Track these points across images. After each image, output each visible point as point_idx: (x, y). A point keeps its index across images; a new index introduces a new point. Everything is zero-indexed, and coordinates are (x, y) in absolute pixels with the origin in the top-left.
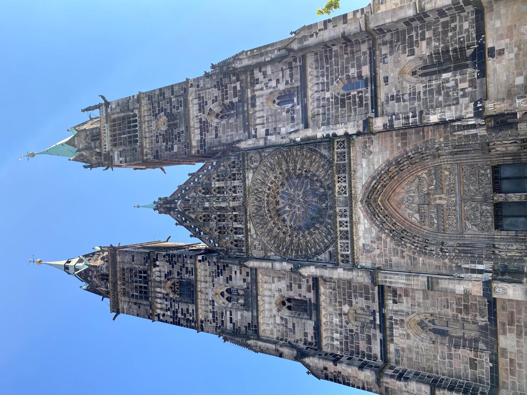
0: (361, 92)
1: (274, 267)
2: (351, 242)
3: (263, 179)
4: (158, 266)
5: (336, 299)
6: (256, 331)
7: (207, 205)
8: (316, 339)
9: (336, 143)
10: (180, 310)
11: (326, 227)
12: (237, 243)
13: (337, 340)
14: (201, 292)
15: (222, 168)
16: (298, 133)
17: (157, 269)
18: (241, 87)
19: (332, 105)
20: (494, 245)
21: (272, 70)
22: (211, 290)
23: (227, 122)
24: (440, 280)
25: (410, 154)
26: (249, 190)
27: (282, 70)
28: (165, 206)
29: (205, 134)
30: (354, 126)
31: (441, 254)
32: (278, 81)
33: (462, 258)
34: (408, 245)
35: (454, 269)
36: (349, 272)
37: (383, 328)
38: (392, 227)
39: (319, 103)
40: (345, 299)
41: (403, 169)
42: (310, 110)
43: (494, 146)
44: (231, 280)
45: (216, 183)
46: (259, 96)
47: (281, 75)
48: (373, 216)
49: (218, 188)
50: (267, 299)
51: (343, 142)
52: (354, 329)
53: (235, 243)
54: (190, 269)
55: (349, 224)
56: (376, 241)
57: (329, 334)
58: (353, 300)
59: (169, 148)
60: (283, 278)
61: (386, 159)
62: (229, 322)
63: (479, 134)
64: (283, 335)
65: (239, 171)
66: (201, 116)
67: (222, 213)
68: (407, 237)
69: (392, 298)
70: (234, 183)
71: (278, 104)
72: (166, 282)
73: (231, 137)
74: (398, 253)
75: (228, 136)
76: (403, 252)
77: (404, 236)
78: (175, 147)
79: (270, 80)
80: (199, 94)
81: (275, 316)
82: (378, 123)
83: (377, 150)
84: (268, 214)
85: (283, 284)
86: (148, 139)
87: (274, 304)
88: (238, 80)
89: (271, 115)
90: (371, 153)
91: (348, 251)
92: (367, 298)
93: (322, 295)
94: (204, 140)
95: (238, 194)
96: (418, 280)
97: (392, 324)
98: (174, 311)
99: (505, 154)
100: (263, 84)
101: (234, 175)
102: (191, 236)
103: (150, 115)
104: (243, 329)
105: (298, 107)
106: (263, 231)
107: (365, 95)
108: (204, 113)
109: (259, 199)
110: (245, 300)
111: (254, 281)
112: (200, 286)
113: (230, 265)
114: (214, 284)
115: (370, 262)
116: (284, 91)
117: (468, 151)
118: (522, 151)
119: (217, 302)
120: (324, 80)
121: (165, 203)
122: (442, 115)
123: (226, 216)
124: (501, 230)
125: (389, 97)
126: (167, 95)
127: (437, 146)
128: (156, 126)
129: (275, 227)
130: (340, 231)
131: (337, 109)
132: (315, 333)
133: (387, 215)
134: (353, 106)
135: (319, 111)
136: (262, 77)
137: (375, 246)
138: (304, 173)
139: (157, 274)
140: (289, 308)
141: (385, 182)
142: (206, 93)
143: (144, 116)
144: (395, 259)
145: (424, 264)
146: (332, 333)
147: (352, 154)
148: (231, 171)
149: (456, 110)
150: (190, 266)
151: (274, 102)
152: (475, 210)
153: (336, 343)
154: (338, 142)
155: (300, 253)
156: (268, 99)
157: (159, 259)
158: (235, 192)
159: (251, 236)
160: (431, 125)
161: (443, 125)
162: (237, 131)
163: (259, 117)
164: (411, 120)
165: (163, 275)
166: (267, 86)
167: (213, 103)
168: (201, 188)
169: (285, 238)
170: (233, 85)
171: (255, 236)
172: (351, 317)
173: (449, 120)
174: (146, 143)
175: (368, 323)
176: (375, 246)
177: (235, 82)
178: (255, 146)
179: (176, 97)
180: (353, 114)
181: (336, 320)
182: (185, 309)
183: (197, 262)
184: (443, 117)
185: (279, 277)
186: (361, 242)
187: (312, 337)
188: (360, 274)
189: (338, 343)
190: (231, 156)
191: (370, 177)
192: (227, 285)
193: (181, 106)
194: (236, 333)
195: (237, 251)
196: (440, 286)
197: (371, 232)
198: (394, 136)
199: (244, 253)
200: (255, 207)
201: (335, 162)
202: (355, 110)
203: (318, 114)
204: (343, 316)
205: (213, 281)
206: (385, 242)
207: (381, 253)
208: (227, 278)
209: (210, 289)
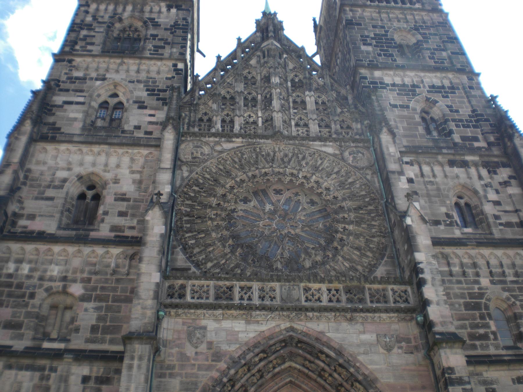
0: (496, 339)
1: (162, 171)
2: (211, 304)
4: (169, 10)
5: (96, 273)
6: (44, 138)
7: (275, 80)
8: (21, 233)
9: (403, 288)
10: (92, 33)
11: (237, 266)
12: (205, 120)
13: (17, 270)
14: (121, 64)
15: (339, 110)
16: (420, 222)
17: (164, 9)
18: (479, 148)
19: (468, 289)
21: (514, 195)
22: (124, 77)
23: (418, 124)
26: (302, 145)
27: (516, 211)
28: (269, 26)
29: (395, 90)
32: (497, 203)
36: (151, 293)
37: (34, 352)
39: (468, 267)
40: (95, 289)
42: (456, 251)
44: (140, 108)
45: (313, 99)
46: (468, 173)
47: (509, 208)
48: (261, 348)
49: (304, 102)
50: (102, 159)
51: (406, 301)
52: (36, 301)
53: (205, 118)
54: (160, 51)
55: (245, 302)
56: (212, 351)
57: (28, 257)
58: (91, 305)
59: (366, 40)
61: (379, 375)
62: (65, 99)
64: (33, 180)
65: (336, 133)
66: (424, 87)
67: (259, 102)
69: (94, 375)
70: (314, 124)
71: (457, 204)
72: (141, 19)
75: (395, 121)
78: (370, 49)
79: (497, 192)
80: (458, 89)
81: (69, 169)
82: (453, 359)
83: (394, 361)
84: (260, 172)
85: (127, 186)
86: (377, 15)
87: (91, 169)
88: (490, 144)
89: (438, 189)
90: (389, 349)
91: (193, 298)
92: (94, 329)
93: (105, 250)
94: (385, 88)
95: (293, 128)
97: (42, 369)
98: (91, 25)
100: (489, 180)
101: (328, 126)
102: (219, 57)
103: (416, 22)
104: (51, 119)
105: (457, 233)
106: (228, 162)
107: (492, 344)
108: (428, 91)
109: (286, 160)
112: (132, 64)
113: (166, 108)
114: (133, 82)
115: (170, 338)
116: (482, 212)
119: (102, 84)
120: (510, 276)
121: (275, 26)
123: (254, 109)
125: (494, 386)
126: (449, 45)
128: (399, 28)
129: (236, 181)
130: (232, 287)
131: (462, 296)
132: (32, 232)
133: (262, 377)
134: (470, 324)
136: (501, 180)
137: (203, 347)
138: (339, 235)
139: (156, 9)
140: (82, 196)
141: (330, 375)
142: (462, 97)
143: (413, 15)
146: (30, 262)
147: (384, 316)
148: (335, 122)
150: (167, 52)
151: (460, 197)
153: (11, 267)
156: (464, 186)
157: (180, 12)
158: (297, 125)
159: (218, 143)
162: (405, 136)
163: (433, 171)
165: (154, 16)
166: (486, 186)
167: (448, 106)
168: (301, 77)
169: (215, 196)
170: (480, 137)
171: (218, 148)
172: (59, 299)
174: (371, 12)
175: (44, 327)
176: (203, 347)
177: (485, 139)
178: (387, 157)
179: (450, 58)
181: (55, 271)
182: (94, 40)
183: (174, 62)
185: (140, 182)
186: (211, 325)
187: (25, 227)
188: (149, 313)
189: (11, 271)
190: (362, 124)
192: (131, 102)
193: (435, 62)
194: (46, 108)
195: (192, 119)
197: (229, 343)
199: (188, 129)
200: (272, 154)
201: (367, 286)
203: (449, 264)
204: (61, 284)
205: (139, 81)
206: (209, 368)
207: (188, 359)
208: (144, 102)
209: (124, 77)
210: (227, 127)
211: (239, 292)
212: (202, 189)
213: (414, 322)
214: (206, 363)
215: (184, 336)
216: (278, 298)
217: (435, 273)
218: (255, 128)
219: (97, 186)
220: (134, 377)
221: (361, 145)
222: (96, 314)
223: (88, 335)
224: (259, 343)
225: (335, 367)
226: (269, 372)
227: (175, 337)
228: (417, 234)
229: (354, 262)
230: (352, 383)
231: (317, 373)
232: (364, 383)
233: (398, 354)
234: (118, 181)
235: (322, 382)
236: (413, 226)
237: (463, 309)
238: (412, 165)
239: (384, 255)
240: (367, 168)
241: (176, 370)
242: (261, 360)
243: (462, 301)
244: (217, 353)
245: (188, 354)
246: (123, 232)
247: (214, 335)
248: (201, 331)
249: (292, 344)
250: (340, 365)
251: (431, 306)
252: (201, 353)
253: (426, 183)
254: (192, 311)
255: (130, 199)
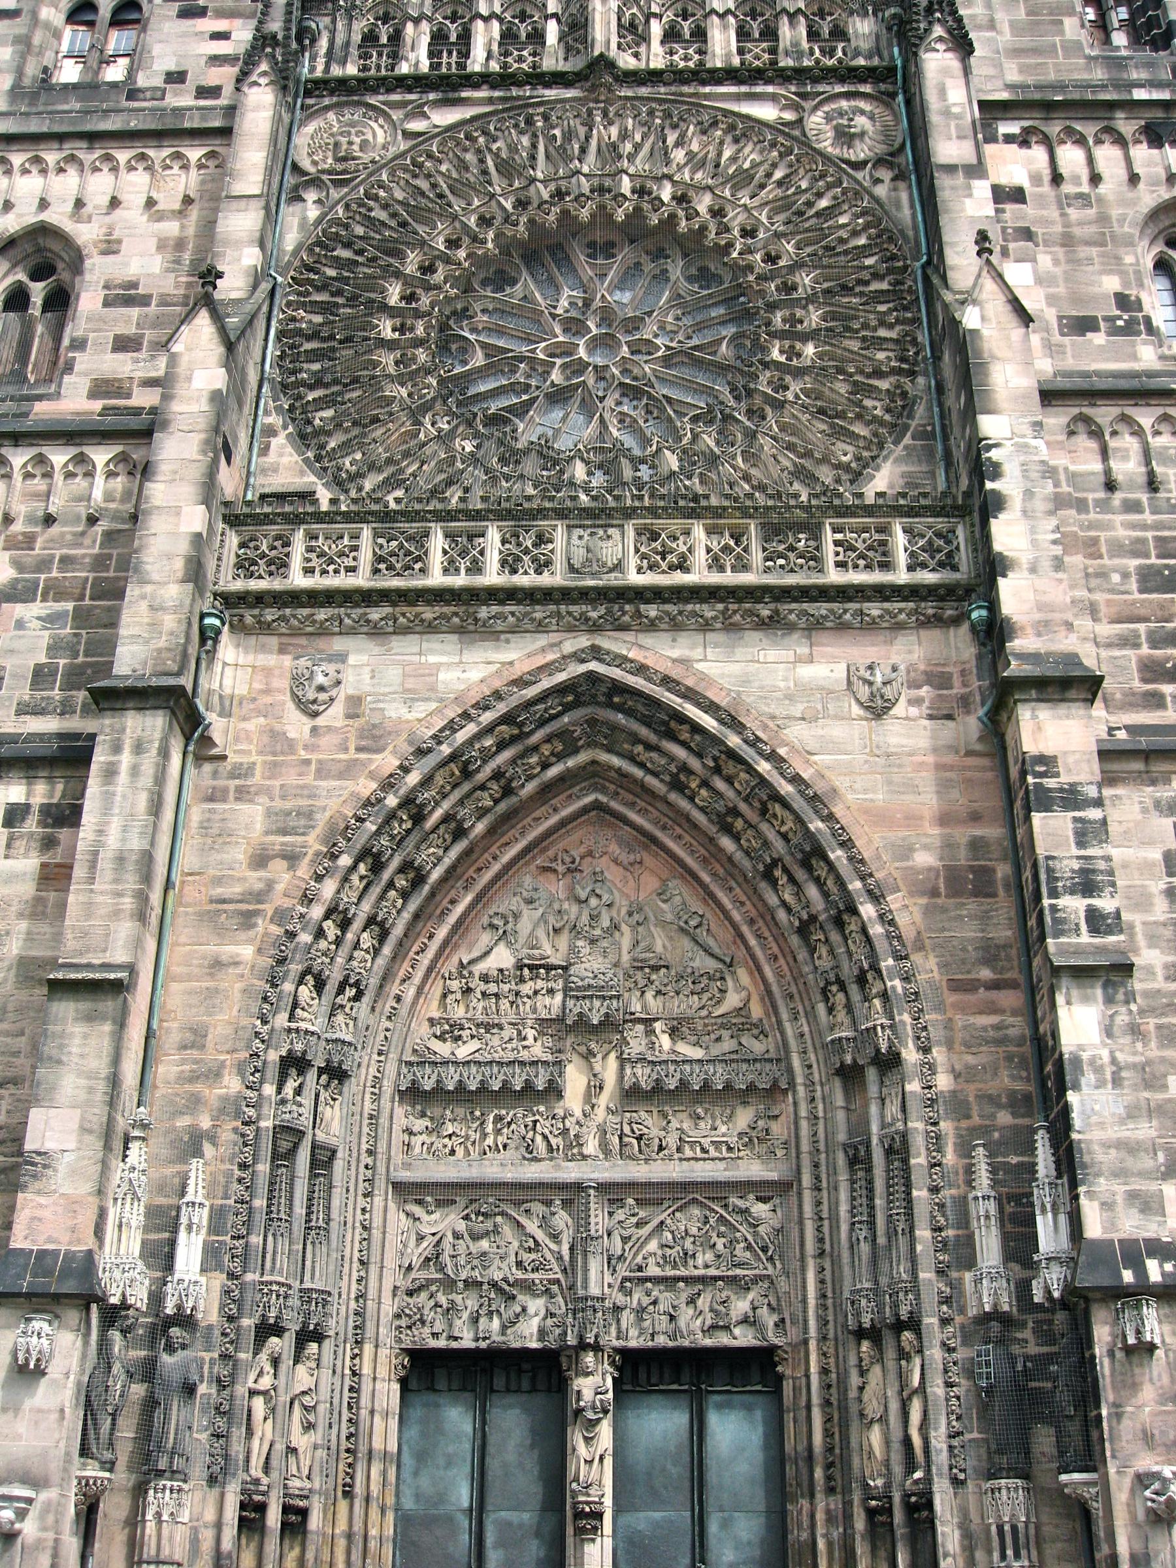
1: (235, 204)
3: (740, 171)
9: (941, 523)
19: (1158, 526)
20: (318, 1336)
24: (107, 1027)
25: (867, 910)
30: (1041, 607)
31: (273, 1056)
33: (243, 1166)
34: (329, 888)
35: (183, 1122)
36: (179, 564)
38: (438, 813)
40: (44, 564)
41: (774, 883)
43: (890, 1354)
48: (502, 708)
50: (67, 184)
55: (460, 580)
60: (177, 262)
61: (841, 783)
63: (968, 1276)
68: (376, 891)
73: (984, 20)
74: (284, 832)
76: (292, 858)
77: (386, 875)
83: (893, 740)
89: (1103, 219)
90: (878, 709)
92: (41, 677)
96: (116, 914)
99: (842, 1414)
110: (69, 89)
111: (169, 123)
115: (242, 690)
117: (872, 1224)
118: (856, 1497)
122: (1098, 1070)
124: (403, 1382)
127: (910, 1055)
135: (1125, 458)
137: (334, 716)
141: (705, 784)
144: (251, 818)
145: (217, 965)
149: (1130, 1148)
152: (527, 1257)
154: (947, 536)
155: (308, 346)
159: (419, 112)
160: (1035, 1024)
161: (1031, 1088)
162: (1016, 52)
163: (1090, 161)
164: (1074, 905)
173: (1066, 1110)
178: (934, 118)
180: (1106, 630)
184: (1088, 1078)
185: (180, 244)
191: (737, 700)
195: (340, 39)
196: (77, 1030)
197: (411, 698)
198: (978, 832)
202: (1130, 642)
206: (348, 771)
207: (291, 745)
210: (450, 53)
211: (445, 552)
212: (360, 252)
213: (965, 628)
214: (343, 756)
215: (283, 683)
216: (559, 564)
217: (1034, 475)
218: (534, 54)
219: (60, 266)
220: (118, 798)
221: (867, 88)
222: (46, 633)
223: (25, 693)
224: (498, 695)
225: (715, 759)
226: (530, 778)
227: (257, 686)
228: (993, 357)
229: (808, 454)
230: (764, 804)
231: (667, 778)
232: (799, 804)
233: (907, 718)
234: (115, 247)
235: (684, 804)
236: (985, 332)
237: (1134, 585)
238: (1025, 143)
239: (906, 428)
240: (879, 162)
241: (257, 778)
242: (501, 746)
243: (1133, 563)
244: (374, 726)
245: (291, 735)
246: (128, 396)
247: (366, 677)
248: (331, 668)
249: (594, 696)
250: (732, 754)
251: (1010, 574)
252: (329, 728)
253: (1064, 202)
254: (305, 612)
255: (151, 296)
